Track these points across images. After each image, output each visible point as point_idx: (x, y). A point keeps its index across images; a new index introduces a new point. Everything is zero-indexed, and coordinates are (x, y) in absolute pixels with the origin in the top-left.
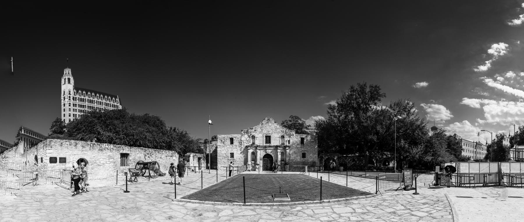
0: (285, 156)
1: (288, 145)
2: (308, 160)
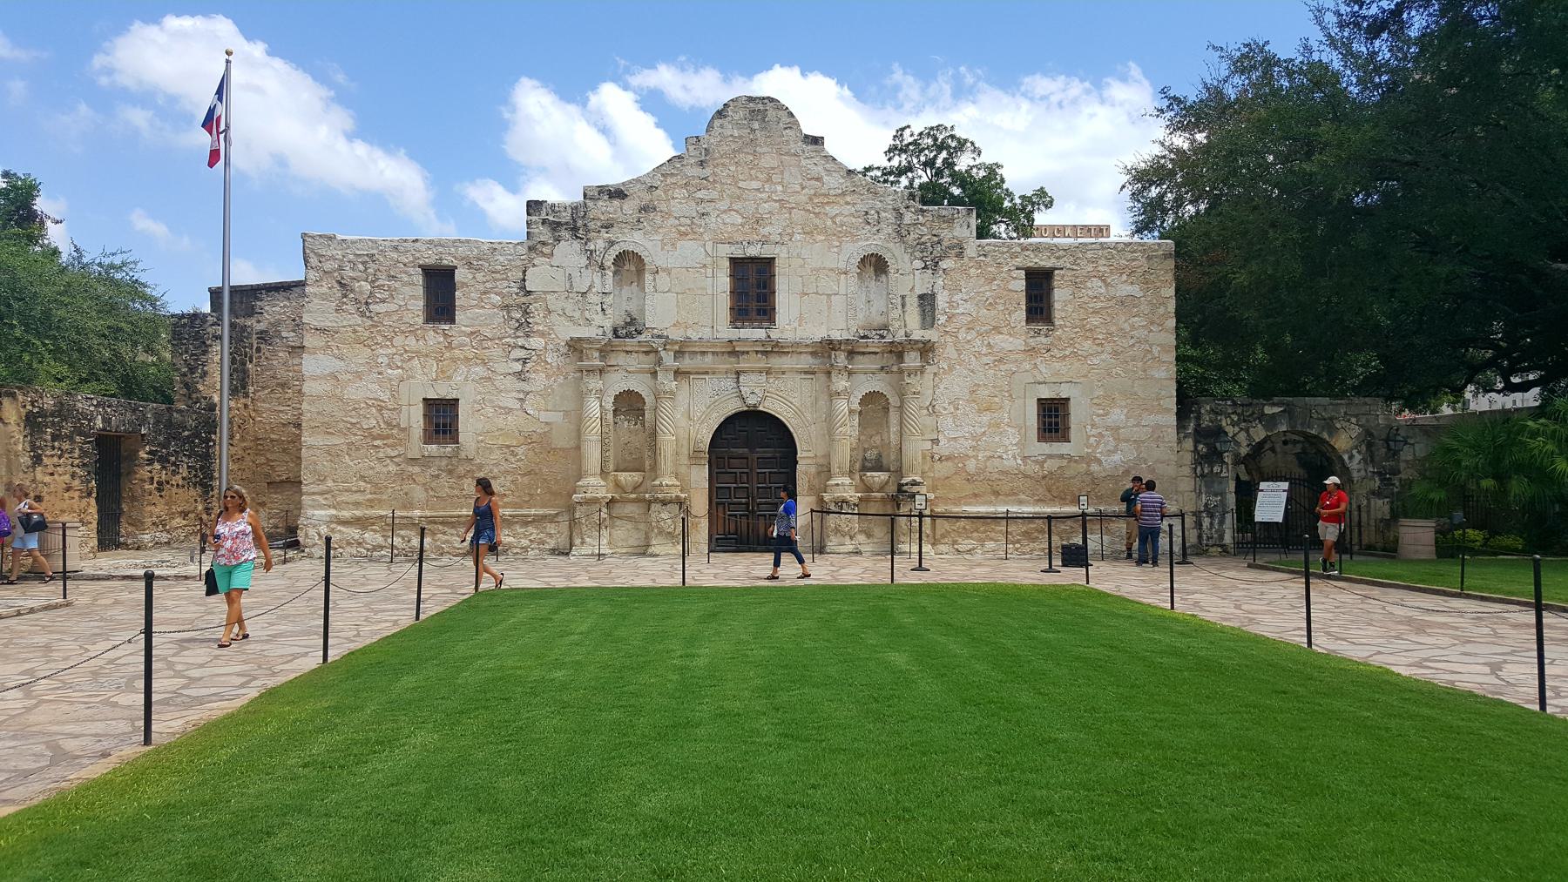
0: (894, 429)
1: (917, 335)
2: (1089, 459)
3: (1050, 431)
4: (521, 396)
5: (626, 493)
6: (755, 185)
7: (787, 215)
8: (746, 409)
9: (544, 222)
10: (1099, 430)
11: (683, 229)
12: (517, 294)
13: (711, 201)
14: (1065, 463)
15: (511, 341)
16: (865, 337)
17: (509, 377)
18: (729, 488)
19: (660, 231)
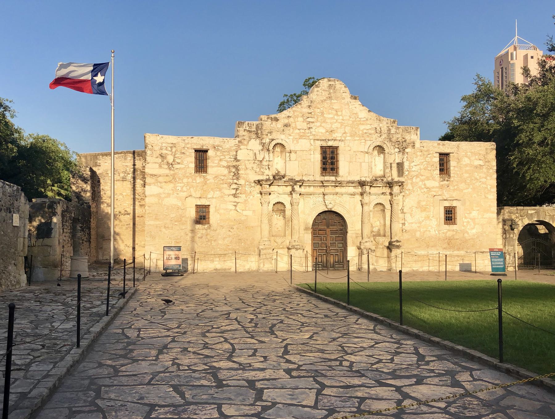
1: (396, 179)
3: (449, 220)
4: (235, 204)
6: (331, 116)
7: (344, 129)
8: (327, 210)
9: (245, 130)
10: (467, 220)
11: (302, 134)
12: (234, 161)
13: (313, 122)
14: (455, 233)
16: (376, 180)
17: (230, 196)
19: (292, 135)
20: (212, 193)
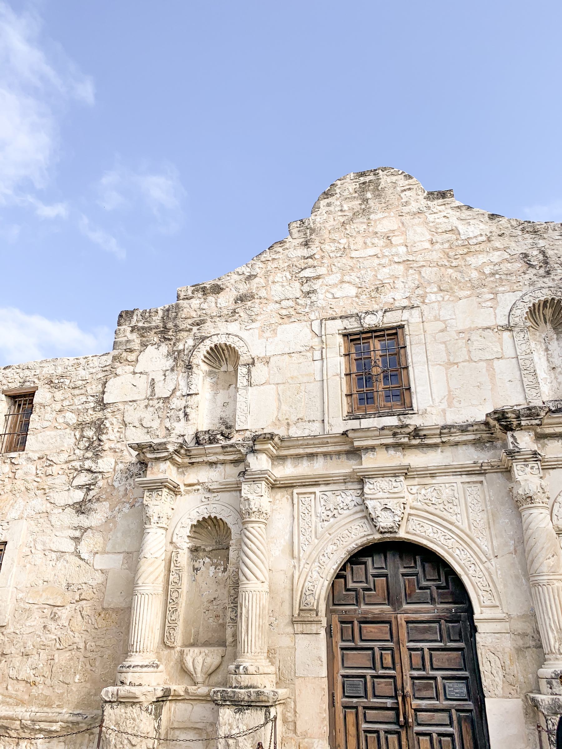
5: (195, 684)
8: (378, 536)
9: (133, 330)
11: (284, 312)
13: (318, 278)
15: (77, 464)
18: (364, 677)
19: (259, 318)
20: (23, 503)
